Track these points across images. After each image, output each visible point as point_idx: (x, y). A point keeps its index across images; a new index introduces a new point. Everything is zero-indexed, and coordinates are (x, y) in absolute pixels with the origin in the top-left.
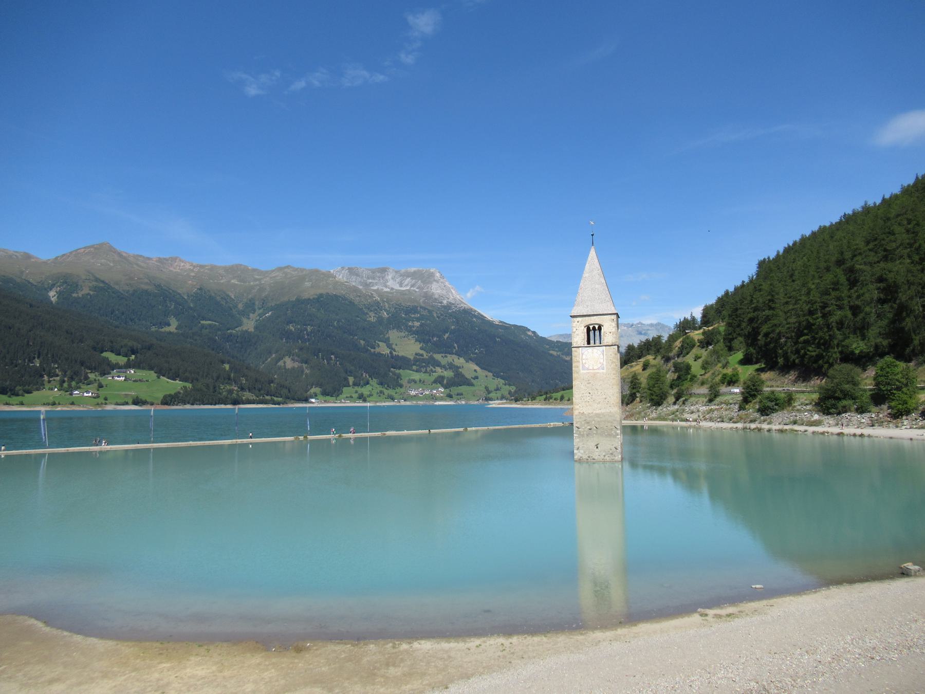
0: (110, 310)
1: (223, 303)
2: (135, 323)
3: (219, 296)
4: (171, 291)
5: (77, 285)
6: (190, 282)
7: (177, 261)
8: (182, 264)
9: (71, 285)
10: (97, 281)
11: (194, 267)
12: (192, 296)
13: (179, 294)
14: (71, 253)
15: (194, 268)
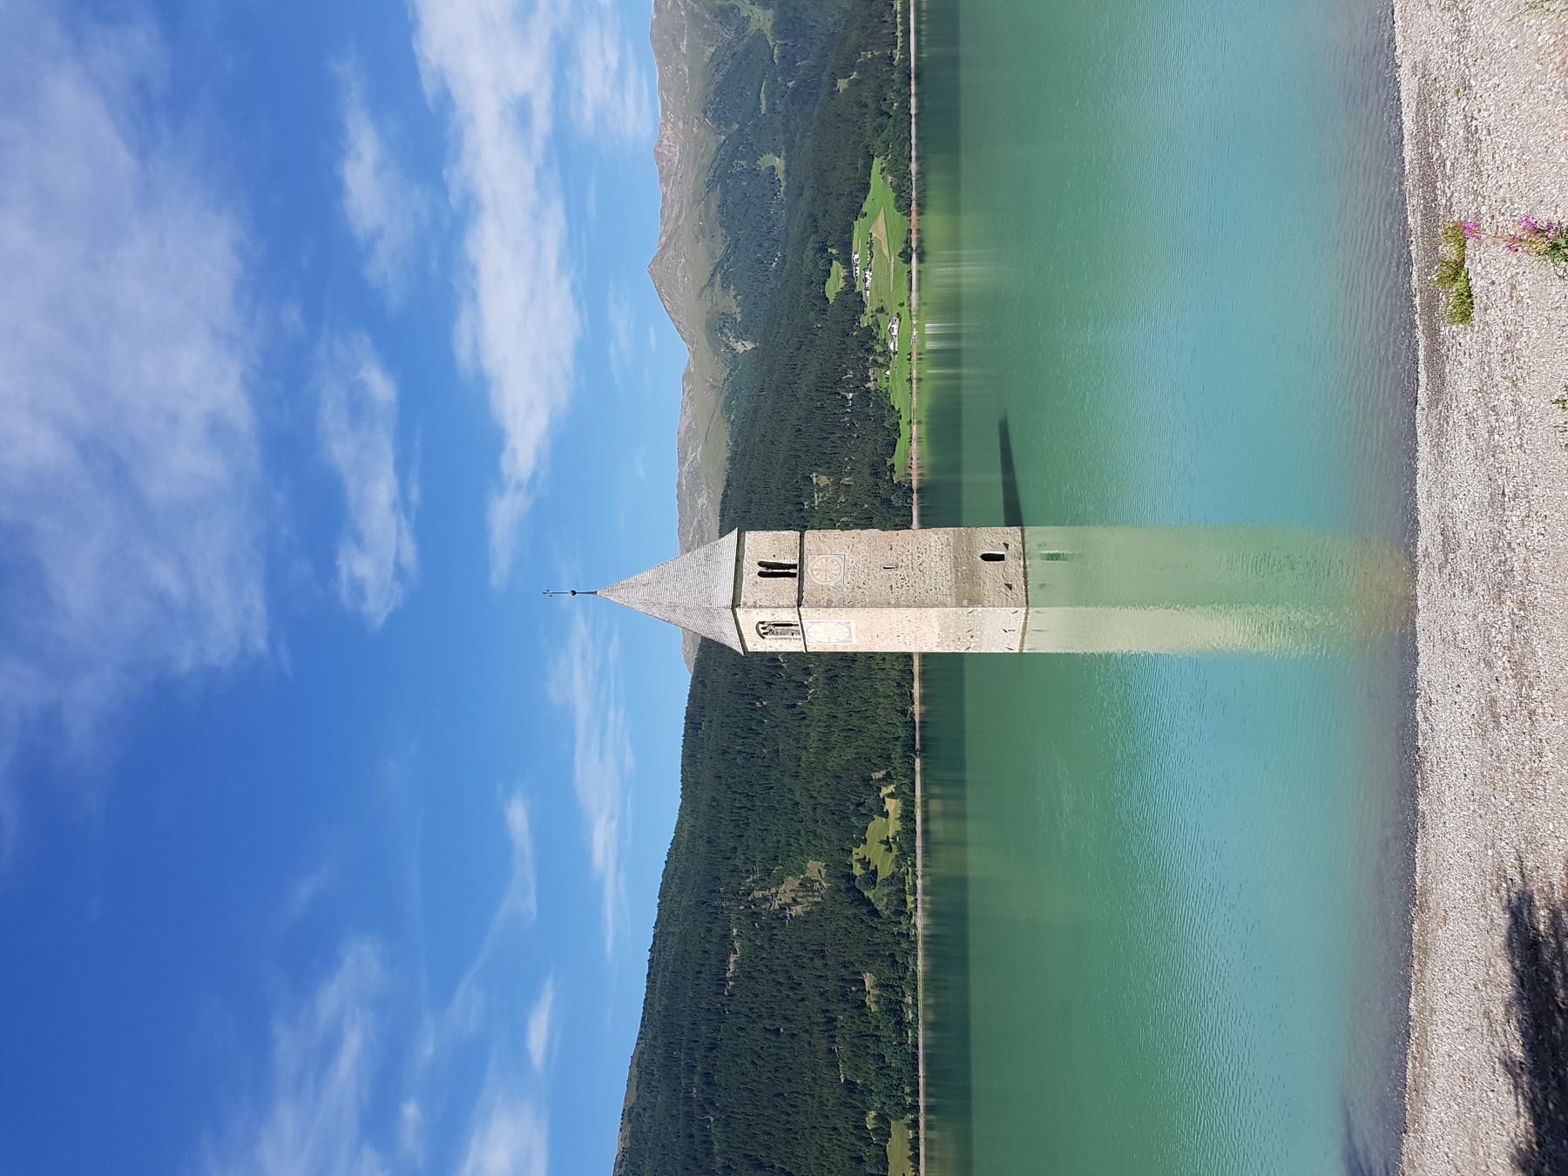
0: (756, 266)
1: (725, 69)
2: (774, 225)
3: (713, 75)
4: (716, 164)
5: (723, 314)
6: (694, 129)
7: (660, 150)
8: (665, 142)
9: (725, 322)
10: (712, 284)
11: (667, 121)
12: (718, 126)
13: (718, 149)
14: (673, 320)
15: (669, 121)
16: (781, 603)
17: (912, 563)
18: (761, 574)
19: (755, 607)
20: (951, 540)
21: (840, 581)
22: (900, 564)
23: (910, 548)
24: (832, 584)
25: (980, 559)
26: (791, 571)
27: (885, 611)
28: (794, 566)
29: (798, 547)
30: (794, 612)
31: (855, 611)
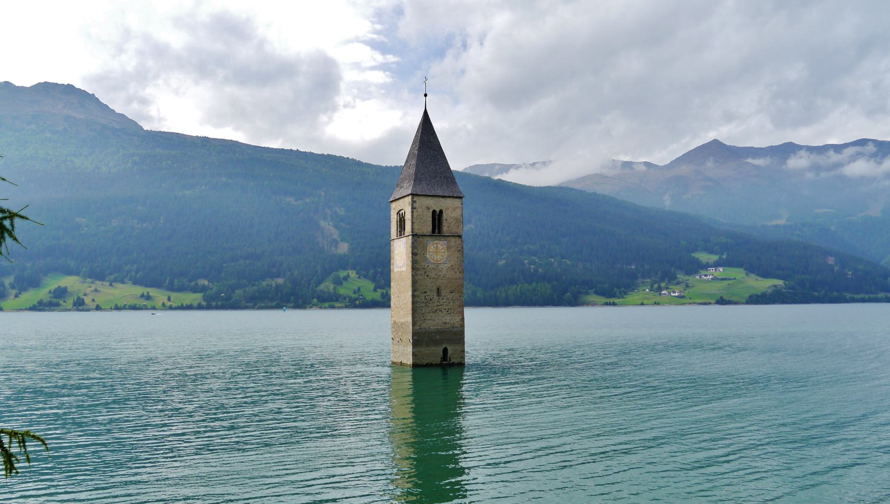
16: (415, 224)
17: (441, 305)
18: (434, 212)
19: (413, 208)
20: (455, 330)
21: (429, 261)
22: (441, 298)
23: (451, 304)
24: (428, 256)
25: (444, 346)
26: (437, 230)
27: (410, 289)
28: (439, 232)
29: (452, 235)
30: (409, 233)
31: (410, 270)
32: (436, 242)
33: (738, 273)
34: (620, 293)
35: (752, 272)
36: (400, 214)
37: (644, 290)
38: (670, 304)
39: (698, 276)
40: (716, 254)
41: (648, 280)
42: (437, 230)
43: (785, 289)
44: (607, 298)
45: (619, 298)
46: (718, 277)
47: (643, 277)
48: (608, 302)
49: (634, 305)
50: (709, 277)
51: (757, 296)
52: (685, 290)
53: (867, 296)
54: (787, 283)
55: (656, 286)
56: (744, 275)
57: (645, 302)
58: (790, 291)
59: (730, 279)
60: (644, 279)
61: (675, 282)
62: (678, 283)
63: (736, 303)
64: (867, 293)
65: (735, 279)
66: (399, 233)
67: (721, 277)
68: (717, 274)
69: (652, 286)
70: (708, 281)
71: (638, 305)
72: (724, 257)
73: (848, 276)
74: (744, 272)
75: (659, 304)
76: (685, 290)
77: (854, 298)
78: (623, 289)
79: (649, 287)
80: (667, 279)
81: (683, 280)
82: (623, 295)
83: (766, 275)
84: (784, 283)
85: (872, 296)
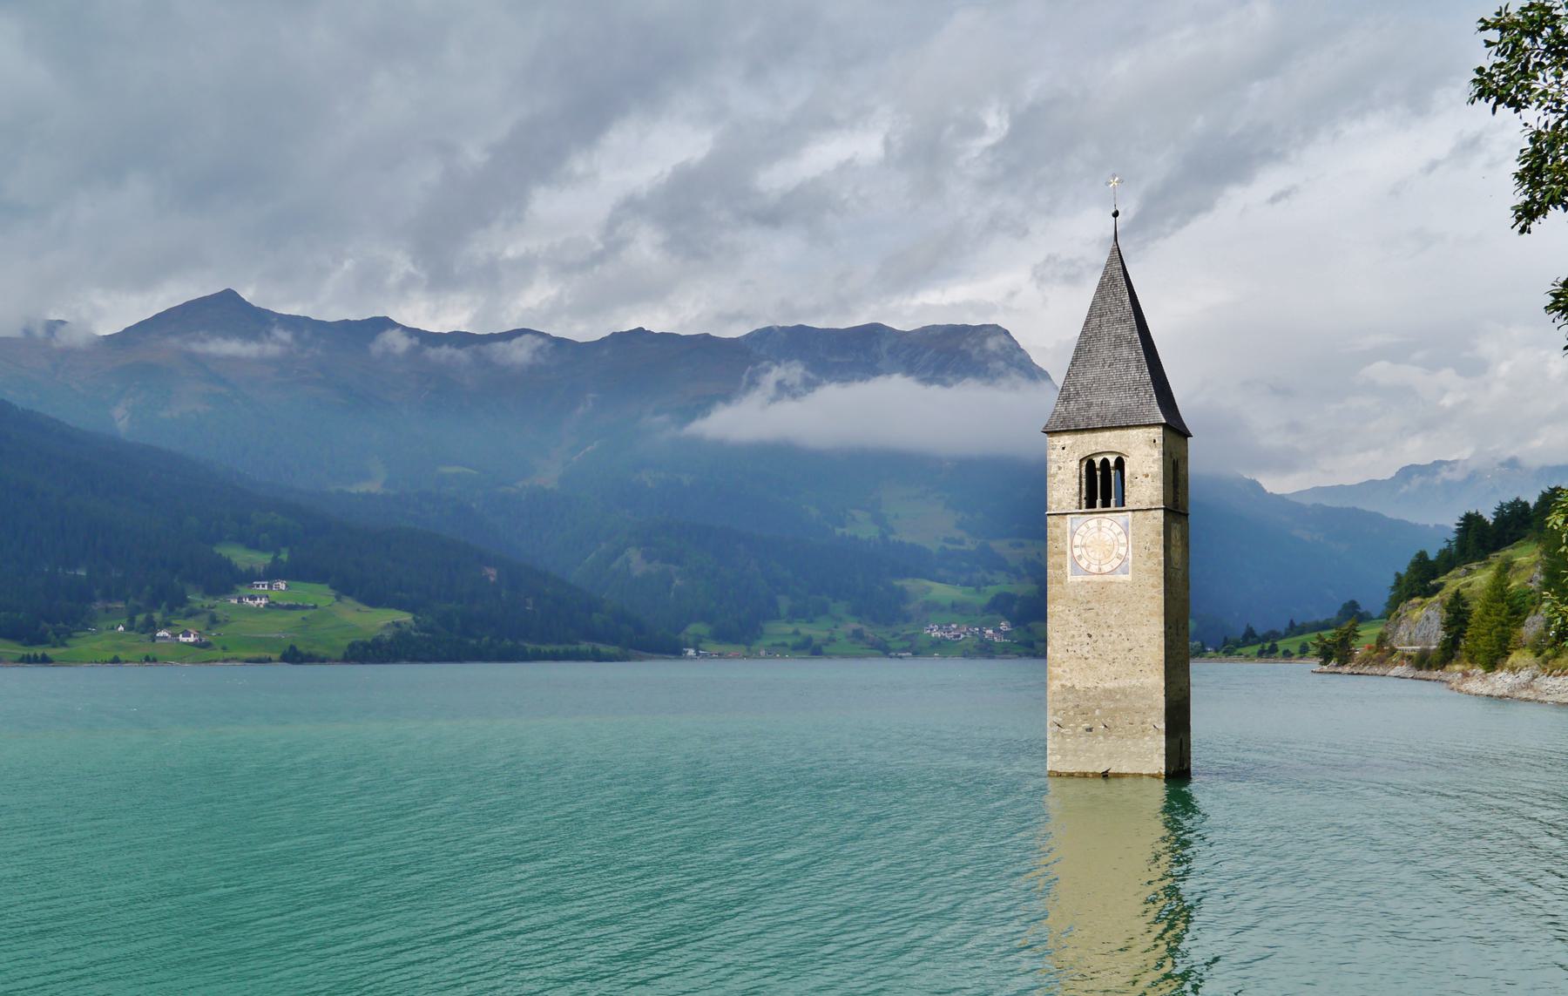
32: (1175, 525)
33: (318, 595)
34: (57, 635)
35: (349, 594)
36: (1091, 464)
37: (113, 628)
38: (182, 660)
39: (234, 598)
40: (264, 550)
41: (120, 605)
42: (1099, 501)
43: (416, 631)
44: (25, 645)
45: (54, 646)
46: (281, 603)
47: (107, 596)
48: (32, 654)
49: (96, 662)
50: (258, 601)
51: (366, 645)
52: (208, 629)
53: (561, 648)
54: (419, 618)
55: (140, 618)
56: (333, 599)
57: (122, 656)
58: (427, 635)
59: (304, 608)
60: (110, 602)
61: (184, 610)
62: (192, 614)
63: (323, 661)
64: (560, 643)
65: (315, 607)
66: (1084, 502)
67: (286, 604)
68: (273, 595)
69: (132, 620)
70: (257, 610)
71: (106, 662)
72: (284, 556)
73: (528, 608)
74: (332, 593)
75: (155, 661)
76: (208, 629)
77: (540, 651)
78: (61, 625)
79: (125, 621)
80: (164, 605)
81: (202, 606)
82: (62, 638)
83: (374, 600)
84: (414, 618)
85: (572, 648)
